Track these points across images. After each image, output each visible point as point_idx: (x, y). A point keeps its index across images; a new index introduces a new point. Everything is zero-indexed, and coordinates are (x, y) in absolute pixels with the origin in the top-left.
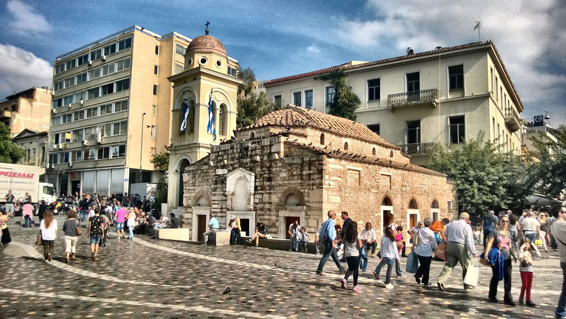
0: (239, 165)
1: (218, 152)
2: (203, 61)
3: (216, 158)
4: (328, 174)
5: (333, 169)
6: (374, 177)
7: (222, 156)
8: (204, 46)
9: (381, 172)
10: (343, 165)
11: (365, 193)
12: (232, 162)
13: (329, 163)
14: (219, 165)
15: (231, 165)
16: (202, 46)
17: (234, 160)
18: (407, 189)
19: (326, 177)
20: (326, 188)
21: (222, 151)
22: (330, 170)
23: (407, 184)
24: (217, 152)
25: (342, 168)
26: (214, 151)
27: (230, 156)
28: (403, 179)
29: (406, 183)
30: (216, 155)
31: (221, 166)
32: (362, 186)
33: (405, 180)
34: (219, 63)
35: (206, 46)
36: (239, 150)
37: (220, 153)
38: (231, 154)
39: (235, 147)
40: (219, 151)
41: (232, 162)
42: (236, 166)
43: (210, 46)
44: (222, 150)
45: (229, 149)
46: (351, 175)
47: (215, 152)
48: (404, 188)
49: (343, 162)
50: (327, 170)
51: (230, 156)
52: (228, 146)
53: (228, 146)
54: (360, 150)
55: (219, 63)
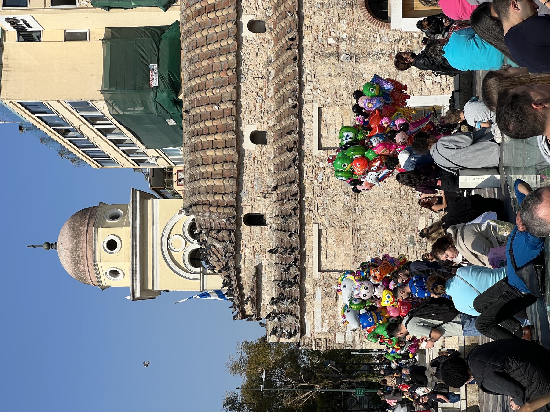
2: (114, 273)
4: (335, 336)
5: (323, 320)
6: (328, 177)
9: (316, 152)
10: (314, 286)
11: (362, 210)
13: (313, 334)
16: (86, 277)
18: (344, 36)
19: (340, 338)
20: (361, 342)
22: (325, 330)
23: (333, 34)
25: (319, 292)
28: (324, 55)
29: (331, 41)
32: (349, 220)
33: (325, 42)
34: (112, 245)
35: (84, 271)
43: (84, 265)
46: (330, 258)
48: (344, 46)
49: (308, 287)
50: (327, 337)
54: (261, 83)
55: (112, 245)
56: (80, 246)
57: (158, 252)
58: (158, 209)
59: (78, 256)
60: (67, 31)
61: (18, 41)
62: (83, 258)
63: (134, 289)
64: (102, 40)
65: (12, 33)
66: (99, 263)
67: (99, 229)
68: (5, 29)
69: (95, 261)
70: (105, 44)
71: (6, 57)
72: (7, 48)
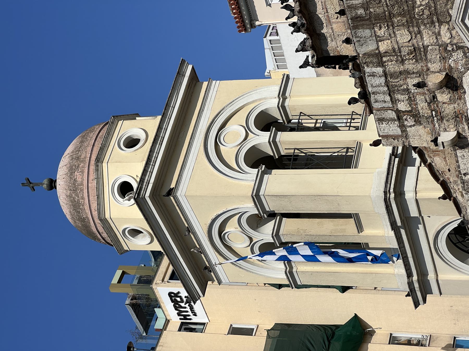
0: (440, 23)
1: (399, 115)
3: (423, 120)
7: (411, 100)
8: (82, 190)
12: (434, 55)
14: (449, 109)
15: (443, 59)
16: (83, 198)
17: (425, 48)
21: (394, 101)
24: (399, 118)
26: (398, 131)
27: (410, 65)
30: (410, 122)
31: (452, 101)
35: (82, 184)
36: (381, 32)
37: (403, 106)
38: (403, 62)
39: (371, 47)
40: (398, 112)
41: (434, 55)
42: (445, 37)
43: (82, 172)
44: (388, 98)
45: (379, 70)
47: (402, 127)
51: (410, 65)
52: (373, 75)
53: (373, 75)
56: (85, 144)
57: (199, 145)
58: (215, 92)
59: (78, 158)
60: (233, 326)
61: (180, 330)
62: (83, 161)
63: (142, 185)
64: (268, 331)
65: (176, 320)
66: (104, 165)
67: (120, 122)
68: (168, 318)
69: (99, 160)
70: (270, 340)
71: (162, 344)
72: (165, 336)
